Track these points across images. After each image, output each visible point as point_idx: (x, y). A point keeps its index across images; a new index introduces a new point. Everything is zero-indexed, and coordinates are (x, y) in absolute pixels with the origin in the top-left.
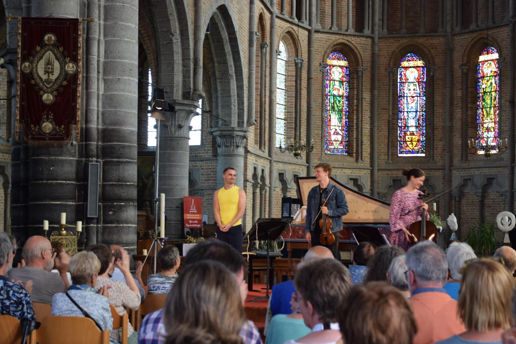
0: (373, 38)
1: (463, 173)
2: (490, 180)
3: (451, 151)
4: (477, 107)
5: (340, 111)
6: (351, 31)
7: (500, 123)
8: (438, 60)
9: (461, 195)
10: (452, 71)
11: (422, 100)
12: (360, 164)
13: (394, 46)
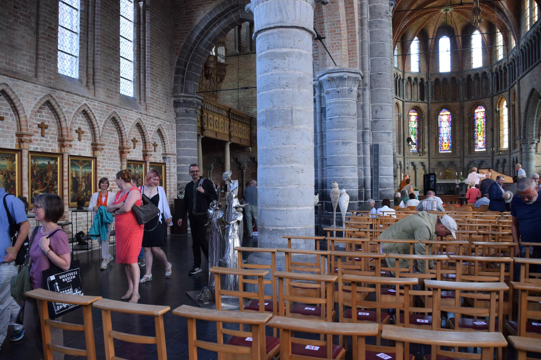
0: (428, 103)
1: (470, 159)
3: (463, 150)
4: (475, 132)
5: (415, 134)
6: (419, 101)
7: (486, 137)
8: (457, 112)
10: (463, 117)
12: (424, 156)
13: (437, 106)
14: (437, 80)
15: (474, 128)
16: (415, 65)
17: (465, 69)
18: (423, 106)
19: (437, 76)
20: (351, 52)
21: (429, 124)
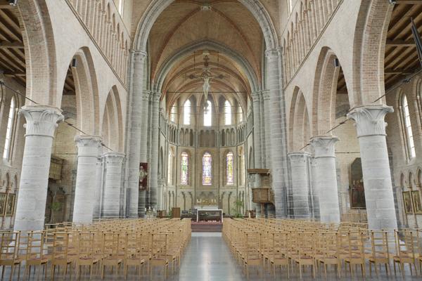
1: (224, 191)
2: (231, 193)
7: (233, 175)
9: (222, 197)
11: (210, 167)
14: (202, 131)
15: (226, 167)
16: (187, 120)
17: (221, 124)
18: (192, 149)
19: (202, 129)
20: (120, 144)
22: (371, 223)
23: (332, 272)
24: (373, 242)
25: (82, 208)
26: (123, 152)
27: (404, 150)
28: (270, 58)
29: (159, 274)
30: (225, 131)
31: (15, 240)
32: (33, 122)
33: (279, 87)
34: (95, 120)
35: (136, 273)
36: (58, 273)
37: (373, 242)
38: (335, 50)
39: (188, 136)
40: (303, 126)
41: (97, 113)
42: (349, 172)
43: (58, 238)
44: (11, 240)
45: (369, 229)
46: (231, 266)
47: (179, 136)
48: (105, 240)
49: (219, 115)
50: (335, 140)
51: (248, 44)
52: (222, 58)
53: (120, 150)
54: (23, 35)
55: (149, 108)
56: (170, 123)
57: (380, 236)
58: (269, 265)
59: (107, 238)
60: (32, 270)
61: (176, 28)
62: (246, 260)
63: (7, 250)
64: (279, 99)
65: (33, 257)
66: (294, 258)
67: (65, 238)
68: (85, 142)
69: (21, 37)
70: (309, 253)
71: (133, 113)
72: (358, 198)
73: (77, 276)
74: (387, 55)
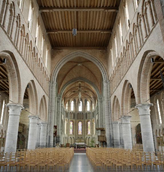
8: (83, 123)
9: (86, 139)
14: (78, 113)
15: (88, 127)
16: (72, 109)
18: (74, 120)
19: (78, 112)
20: (46, 118)
21: (76, 126)
22: (144, 149)
23: (129, 168)
24: (145, 157)
25: (31, 144)
26: (47, 121)
27: (157, 121)
28: (105, 84)
29: (61, 169)
30: (87, 113)
31: (5, 156)
32: (12, 110)
33: (108, 96)
34: (36, 109)
35: (52, 169)
36: (22, 169)
37: (145, 157)
38: (130, 81)
39: (73, 115)
40: (118, 111)
41: (37, 106)
42: (136, 129)
43: (22, 155)
44: (4, 156)
45: (144, 152)
46: (89, 166)
47: (69, 115)
48: (40, 156)
49: (85, 107)
50: (130, 117)
51: (96, 79)
52: (86, 84)
53: (46, 121)
54: (8, 75)
55: (57, 104)
56: (66, 110)
57: (148, 154)
58: (104, 166)
59: (41, 155)
60: (12, 168)
61: (68, 73)
62: (95, 164)
63: (2, 160)
64: (108, 101)
65: (12, 163)
66: (114, 163)
67: (24, 155)
68: (32, 117)
69: (7, 76)
70: (120, 161)
71: (51, 106)
72: (139, 140)
73: (29, 170)
74: (150, 83)
